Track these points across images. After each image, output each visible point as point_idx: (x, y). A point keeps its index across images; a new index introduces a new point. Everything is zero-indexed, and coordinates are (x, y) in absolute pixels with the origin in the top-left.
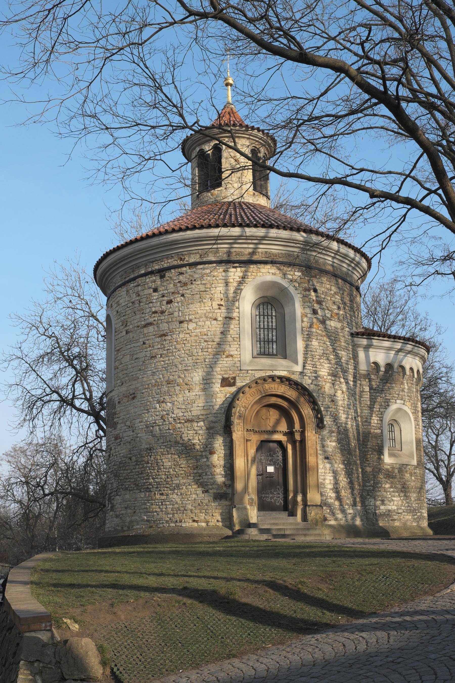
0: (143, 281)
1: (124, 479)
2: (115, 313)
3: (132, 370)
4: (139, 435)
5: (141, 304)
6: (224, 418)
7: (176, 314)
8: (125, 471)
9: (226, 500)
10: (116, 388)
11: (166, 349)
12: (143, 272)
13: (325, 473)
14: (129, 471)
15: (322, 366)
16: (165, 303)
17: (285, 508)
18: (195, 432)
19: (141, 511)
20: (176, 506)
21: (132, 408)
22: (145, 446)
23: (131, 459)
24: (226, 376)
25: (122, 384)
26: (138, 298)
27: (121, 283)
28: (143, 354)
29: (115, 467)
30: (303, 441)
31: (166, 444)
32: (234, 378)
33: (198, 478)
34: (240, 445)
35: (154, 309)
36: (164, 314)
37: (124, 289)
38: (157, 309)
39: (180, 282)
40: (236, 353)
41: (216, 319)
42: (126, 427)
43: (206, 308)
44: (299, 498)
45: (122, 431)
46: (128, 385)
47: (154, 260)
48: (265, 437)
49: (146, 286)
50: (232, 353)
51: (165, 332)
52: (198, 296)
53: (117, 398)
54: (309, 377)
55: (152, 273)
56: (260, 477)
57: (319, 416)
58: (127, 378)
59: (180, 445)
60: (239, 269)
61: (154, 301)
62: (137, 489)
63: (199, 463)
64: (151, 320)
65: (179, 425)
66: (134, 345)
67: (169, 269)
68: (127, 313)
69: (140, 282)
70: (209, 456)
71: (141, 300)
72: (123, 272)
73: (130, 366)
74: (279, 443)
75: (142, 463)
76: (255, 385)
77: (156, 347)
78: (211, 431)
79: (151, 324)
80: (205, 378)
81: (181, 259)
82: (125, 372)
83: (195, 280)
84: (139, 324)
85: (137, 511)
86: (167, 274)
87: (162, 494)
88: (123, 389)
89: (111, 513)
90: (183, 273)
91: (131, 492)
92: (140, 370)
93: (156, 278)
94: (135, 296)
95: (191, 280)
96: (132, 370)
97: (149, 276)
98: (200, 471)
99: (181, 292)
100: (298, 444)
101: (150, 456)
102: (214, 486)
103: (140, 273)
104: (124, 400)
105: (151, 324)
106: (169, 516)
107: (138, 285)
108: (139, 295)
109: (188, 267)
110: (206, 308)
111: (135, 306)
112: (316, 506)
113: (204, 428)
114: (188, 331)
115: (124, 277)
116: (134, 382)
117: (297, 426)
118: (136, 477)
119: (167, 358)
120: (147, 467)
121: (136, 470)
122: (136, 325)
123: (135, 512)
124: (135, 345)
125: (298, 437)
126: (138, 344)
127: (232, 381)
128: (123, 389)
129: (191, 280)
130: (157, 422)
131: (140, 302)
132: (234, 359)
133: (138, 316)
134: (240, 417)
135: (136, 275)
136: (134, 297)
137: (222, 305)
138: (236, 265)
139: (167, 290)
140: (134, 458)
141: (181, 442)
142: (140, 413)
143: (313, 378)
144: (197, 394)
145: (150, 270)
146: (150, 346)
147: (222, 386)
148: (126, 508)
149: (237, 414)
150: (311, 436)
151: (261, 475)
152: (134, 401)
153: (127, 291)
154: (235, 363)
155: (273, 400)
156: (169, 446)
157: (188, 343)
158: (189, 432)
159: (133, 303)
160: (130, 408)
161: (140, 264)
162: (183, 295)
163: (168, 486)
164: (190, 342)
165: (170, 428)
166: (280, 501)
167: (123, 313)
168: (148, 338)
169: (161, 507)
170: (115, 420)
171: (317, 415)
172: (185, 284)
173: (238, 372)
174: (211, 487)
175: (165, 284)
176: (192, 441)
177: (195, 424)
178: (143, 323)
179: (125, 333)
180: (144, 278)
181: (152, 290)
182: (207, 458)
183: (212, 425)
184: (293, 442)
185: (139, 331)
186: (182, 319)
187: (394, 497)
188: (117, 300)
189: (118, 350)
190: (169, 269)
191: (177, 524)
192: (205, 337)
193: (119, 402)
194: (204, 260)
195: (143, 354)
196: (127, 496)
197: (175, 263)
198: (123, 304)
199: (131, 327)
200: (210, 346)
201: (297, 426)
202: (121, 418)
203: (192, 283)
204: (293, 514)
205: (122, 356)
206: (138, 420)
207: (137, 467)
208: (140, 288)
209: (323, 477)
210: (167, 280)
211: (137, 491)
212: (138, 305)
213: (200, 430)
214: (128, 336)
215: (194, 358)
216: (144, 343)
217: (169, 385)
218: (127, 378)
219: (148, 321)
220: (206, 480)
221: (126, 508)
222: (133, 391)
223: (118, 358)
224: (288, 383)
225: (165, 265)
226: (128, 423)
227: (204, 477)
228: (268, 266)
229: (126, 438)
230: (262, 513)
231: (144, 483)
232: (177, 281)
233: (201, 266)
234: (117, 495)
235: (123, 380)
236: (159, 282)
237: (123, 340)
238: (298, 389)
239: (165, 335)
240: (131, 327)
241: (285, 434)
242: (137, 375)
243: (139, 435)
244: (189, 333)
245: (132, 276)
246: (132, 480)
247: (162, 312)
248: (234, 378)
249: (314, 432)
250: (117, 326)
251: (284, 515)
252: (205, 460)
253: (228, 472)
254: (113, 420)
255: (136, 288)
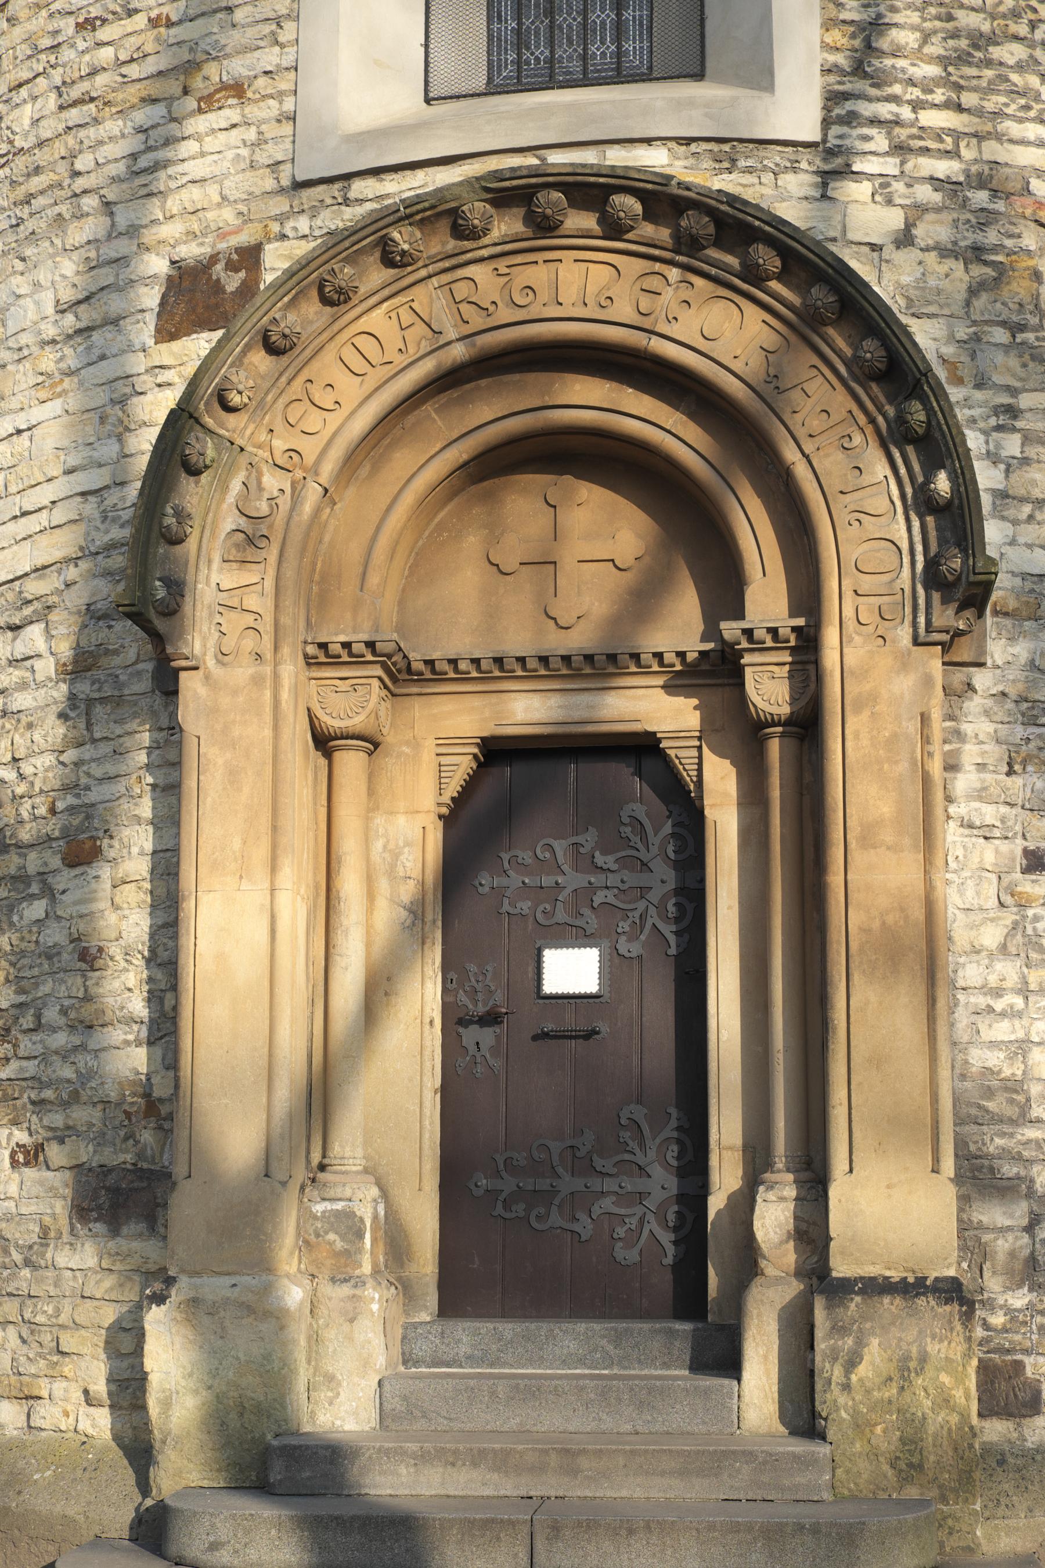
13: (1024, 991)
15: (1016, 92)
17: (688, 1299)
30: (807, 725)
40: (270, 57)
44: (773, 1218)
48: (527, 710)
50: (238, 67)
54: (884, 182)
56: (487, 1036)
57: (942, 483)
70: (63, 880)
74: (643, 749)
76: (377, 275)
100: (774, 747)
112: (912, 1288)
117: (767, 601)
125: (768, 690)
132: (254, 112)
134: (250, 540)
143: (925, 193)
149: (230, 521)
150: (877, 674)
151: (491, 1019)
154: (261, 142)
155: (587, 400)
166: (648, 1236)
171: (929, 478)
173: (280, 205)
182: (49, 892)
184: (741, 732)
201: (767, 601)
204: (723, 1358)
209: (1002, 1031)
224: (664, 234)
230: (466, 1334)
238: (754, 275)
241: (687, 676)
249: (904, 635)
251: (657, 1353)
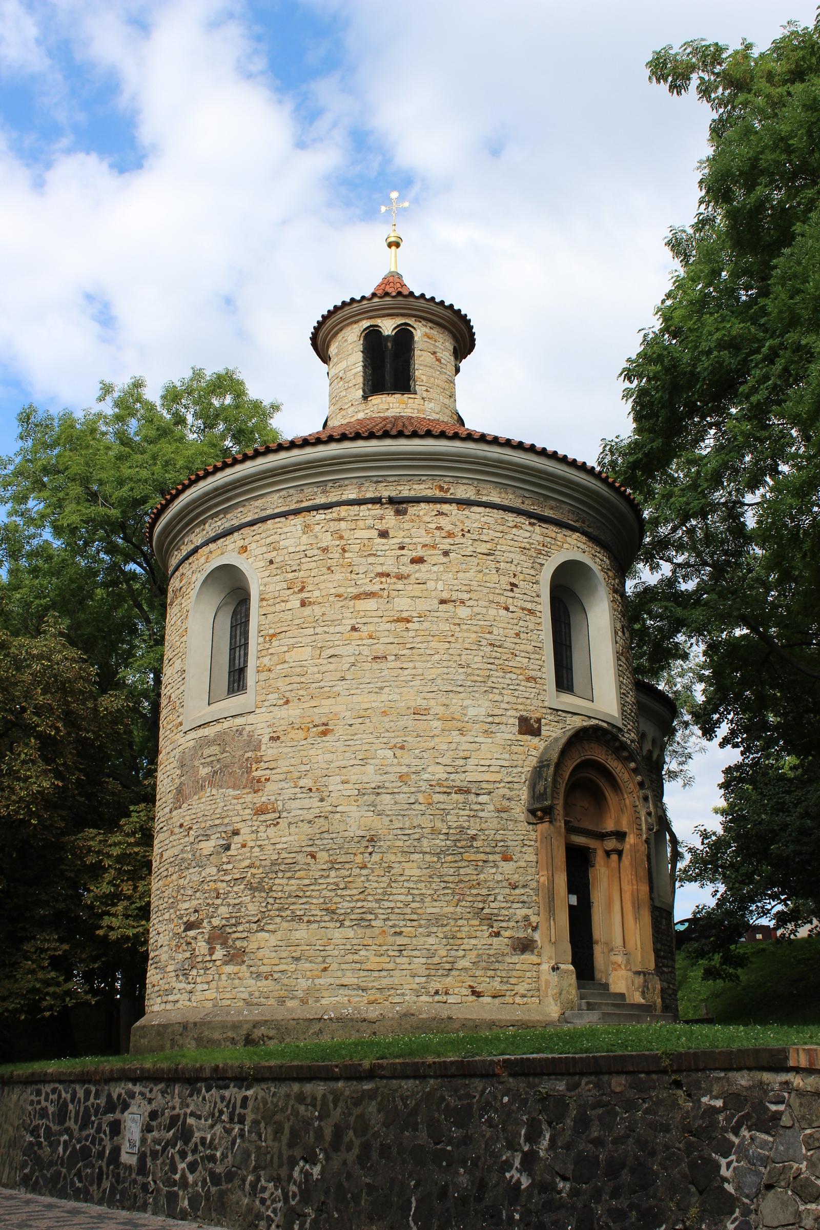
0: (352, 513)
1: (290, 896)
2: (262, 564)
3: (319, 676)
4: (338, 809)
5: (347, 555)
6: (526, 793)
7: (431, 585)
8: (293, 882)
9: (532, 951)
10: (263, 710)
11: (408, 646)
12: (353, 496)
14: (307, 882)
16: (406, 560)
18: (472, 813)
19: (344, 966)
20: (436, 960)
21: (320, 752)
22: (354, 830)
23: (314, 857)
24: (525, 713)
25: (287, 702)
26: (338, 543)
27: (287, 509)
28: (350, 650)
29: (253, 871)
31: (411, 832)
32: (539, 721)
33: (481, 905)
34: (558, 847)
35: (379, 569)
36: (406, 581)
37: (298, 521)
38: (385, 569)
39: (438, 528)
40: (539, 674)
41: (507, 609)
42: (298, 790)
43: (488, 585)
45: (286, 797)
46: (306, 705)
47: (380, 479)
49: (361, 523)
51: (405, 615)
52: (476, 561)
53: (270, 730)
55: (377, 501)
58: (301, 692)
59: (441, 837)
60: (537, 529)
61: (379, 553)
62: (332, 920)
63: (482, 876)
64: (376, 588)
65: (442, 798)
66: (325, 629)
67: (417, 501)
68: (304, 567)
69: (343, 514)
71: (347, 548)
72: (292, 491)
73: (315, 669)
75: (347, 866)
77: (382, 640)
78: (504, 815)
79: (371, 595)
80: (491, 713)
81: (441, 489)
82: (298, 679)
83: (469, 531)
84: (341, 590)
85: (334, 966)
86: (412, 510)
87: (401, 933)
88: (293, 712)
89: (229, 969)
90: (443, 514)
91: (315, 926)
92: (343, 679)
93: (389, 512)
94: (330, 538)
95: (462, 530)
96: (319, 676)
97: (370, 506)
98: (484, 892)
99: (442, 547)
101: (371, 854)
102: (511, 924)
103: (344, 497)
104: (290, 736)
105: (371, 595)
106: (417, 980)
107: (340, 520)
108: (341, 538)
109: (454, 506)
110: (488, 585)
111: (331, 556)
113: (491, 807)
114: (457, 621)
115: (295, 499)
116: (324, 702)
118: (329, 894)
119: (411, 665)
120: (361, 875)
121: (328, 880)
122: (333, 591)
123: (325, 969)
124: (331, 630)
126: (338, 629)
127: (536, 726)
128: (293, 712)
129: (462, 530)
130: (387, 785)
131: (344, 551)
132: (538, 686)
133: (338, 576)
135: (334, 500)
136: (327, 540)
137: (516, 586)
138: (532, 521)
139: (411, 537)
140: (323, 856)
141: (444, 831)
142: (342, 764)
144: (477, 740)
145: (369, 495)
146: (371, 637)
147: (521, 732)
148: (298, 959)
152: (324, 739)
153: (307, 528)
156: (417, 836)
157: (456, 642)
158: (462, 813)
159: (325, 550)
160: (312, 752)
161: (346, 482)
162: (446, 553)
163: (415, 917)
164: (460, 640)
165: (421, 800)
167: (291, 566)
168: (364, 620)
169: (398, 960)
170: (255, 774)
172: (450, 535)
173: (544, 711)
174: (504, 924)
175: (406, 526)
176: (469, 832)
177: (472, 797)
178: (349, 590)
179: (297, 604)
180: (356, 508)
181: (375, 533)
183: (506, 803)
185: (342, 604)
186: (445, 595)
187: (664, 966)
188: (268, 541)
189: (274, 635)
190: (417, 501)
191: (437, 998)
192: (488, 636)
193: (272, 738)
194: (484, 499)
195: (350, 650)
196: (298, 934)
197: (429, 493)
198: (291, 550)
199: (317, 593)
200: (498, 655)
202: (278, 770)
203: (463, 535)
205: (285, 649)
206: (338, 779)
207: (333, 873)
208: (343, 524)
210: (413, 521)
211: (332, 925)
212: (337, 555)
213: (483, 810)
214: (307, 611)
215: (469, 671)
216: (354, 629)
217: (417, 717)
218: (301, 692)
219: (369, 588)
220: (496, 911)
221: (298, 959)
222: (324, 720)
223: (270, 651)
225: (406, 494)
226: (302, 783)
227: (492, 905)
228: (576, 535)
229: (300, 812)
231: (353, 908)
232: (433, 526)
233: (481, 509)
234: (262, 930)
235: (287, 695)
236: (390, 519)
237: (290, 617)
239: (408, 621)
240: (317, 593)
242: (335, 689)
243: (338, 809)
244: (459, 625)
245: (321, 500)
246: (315, 901)
247: (400, 577)
248: (539, 721)
250: (271, 588)
252: (494, 870)
253: (534, 898)
254: (249, 771)
255: (332, 523)
